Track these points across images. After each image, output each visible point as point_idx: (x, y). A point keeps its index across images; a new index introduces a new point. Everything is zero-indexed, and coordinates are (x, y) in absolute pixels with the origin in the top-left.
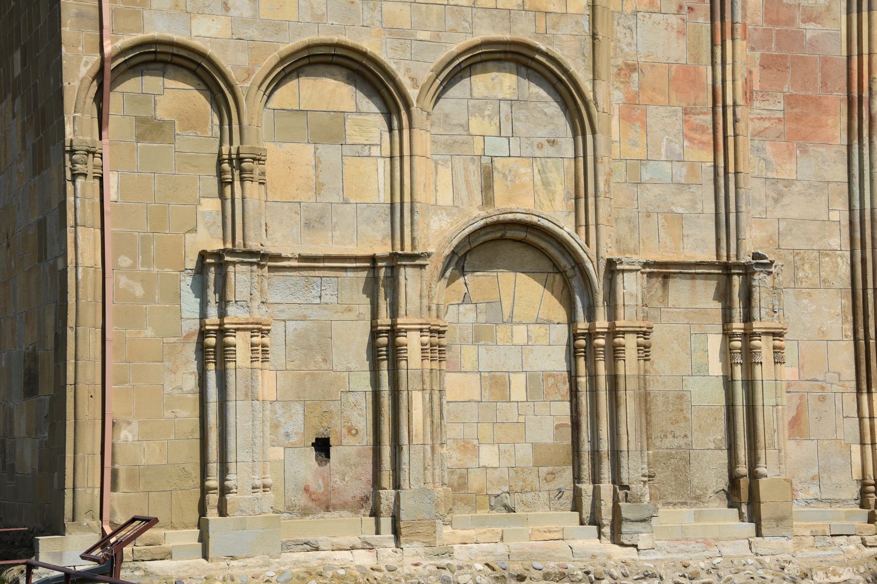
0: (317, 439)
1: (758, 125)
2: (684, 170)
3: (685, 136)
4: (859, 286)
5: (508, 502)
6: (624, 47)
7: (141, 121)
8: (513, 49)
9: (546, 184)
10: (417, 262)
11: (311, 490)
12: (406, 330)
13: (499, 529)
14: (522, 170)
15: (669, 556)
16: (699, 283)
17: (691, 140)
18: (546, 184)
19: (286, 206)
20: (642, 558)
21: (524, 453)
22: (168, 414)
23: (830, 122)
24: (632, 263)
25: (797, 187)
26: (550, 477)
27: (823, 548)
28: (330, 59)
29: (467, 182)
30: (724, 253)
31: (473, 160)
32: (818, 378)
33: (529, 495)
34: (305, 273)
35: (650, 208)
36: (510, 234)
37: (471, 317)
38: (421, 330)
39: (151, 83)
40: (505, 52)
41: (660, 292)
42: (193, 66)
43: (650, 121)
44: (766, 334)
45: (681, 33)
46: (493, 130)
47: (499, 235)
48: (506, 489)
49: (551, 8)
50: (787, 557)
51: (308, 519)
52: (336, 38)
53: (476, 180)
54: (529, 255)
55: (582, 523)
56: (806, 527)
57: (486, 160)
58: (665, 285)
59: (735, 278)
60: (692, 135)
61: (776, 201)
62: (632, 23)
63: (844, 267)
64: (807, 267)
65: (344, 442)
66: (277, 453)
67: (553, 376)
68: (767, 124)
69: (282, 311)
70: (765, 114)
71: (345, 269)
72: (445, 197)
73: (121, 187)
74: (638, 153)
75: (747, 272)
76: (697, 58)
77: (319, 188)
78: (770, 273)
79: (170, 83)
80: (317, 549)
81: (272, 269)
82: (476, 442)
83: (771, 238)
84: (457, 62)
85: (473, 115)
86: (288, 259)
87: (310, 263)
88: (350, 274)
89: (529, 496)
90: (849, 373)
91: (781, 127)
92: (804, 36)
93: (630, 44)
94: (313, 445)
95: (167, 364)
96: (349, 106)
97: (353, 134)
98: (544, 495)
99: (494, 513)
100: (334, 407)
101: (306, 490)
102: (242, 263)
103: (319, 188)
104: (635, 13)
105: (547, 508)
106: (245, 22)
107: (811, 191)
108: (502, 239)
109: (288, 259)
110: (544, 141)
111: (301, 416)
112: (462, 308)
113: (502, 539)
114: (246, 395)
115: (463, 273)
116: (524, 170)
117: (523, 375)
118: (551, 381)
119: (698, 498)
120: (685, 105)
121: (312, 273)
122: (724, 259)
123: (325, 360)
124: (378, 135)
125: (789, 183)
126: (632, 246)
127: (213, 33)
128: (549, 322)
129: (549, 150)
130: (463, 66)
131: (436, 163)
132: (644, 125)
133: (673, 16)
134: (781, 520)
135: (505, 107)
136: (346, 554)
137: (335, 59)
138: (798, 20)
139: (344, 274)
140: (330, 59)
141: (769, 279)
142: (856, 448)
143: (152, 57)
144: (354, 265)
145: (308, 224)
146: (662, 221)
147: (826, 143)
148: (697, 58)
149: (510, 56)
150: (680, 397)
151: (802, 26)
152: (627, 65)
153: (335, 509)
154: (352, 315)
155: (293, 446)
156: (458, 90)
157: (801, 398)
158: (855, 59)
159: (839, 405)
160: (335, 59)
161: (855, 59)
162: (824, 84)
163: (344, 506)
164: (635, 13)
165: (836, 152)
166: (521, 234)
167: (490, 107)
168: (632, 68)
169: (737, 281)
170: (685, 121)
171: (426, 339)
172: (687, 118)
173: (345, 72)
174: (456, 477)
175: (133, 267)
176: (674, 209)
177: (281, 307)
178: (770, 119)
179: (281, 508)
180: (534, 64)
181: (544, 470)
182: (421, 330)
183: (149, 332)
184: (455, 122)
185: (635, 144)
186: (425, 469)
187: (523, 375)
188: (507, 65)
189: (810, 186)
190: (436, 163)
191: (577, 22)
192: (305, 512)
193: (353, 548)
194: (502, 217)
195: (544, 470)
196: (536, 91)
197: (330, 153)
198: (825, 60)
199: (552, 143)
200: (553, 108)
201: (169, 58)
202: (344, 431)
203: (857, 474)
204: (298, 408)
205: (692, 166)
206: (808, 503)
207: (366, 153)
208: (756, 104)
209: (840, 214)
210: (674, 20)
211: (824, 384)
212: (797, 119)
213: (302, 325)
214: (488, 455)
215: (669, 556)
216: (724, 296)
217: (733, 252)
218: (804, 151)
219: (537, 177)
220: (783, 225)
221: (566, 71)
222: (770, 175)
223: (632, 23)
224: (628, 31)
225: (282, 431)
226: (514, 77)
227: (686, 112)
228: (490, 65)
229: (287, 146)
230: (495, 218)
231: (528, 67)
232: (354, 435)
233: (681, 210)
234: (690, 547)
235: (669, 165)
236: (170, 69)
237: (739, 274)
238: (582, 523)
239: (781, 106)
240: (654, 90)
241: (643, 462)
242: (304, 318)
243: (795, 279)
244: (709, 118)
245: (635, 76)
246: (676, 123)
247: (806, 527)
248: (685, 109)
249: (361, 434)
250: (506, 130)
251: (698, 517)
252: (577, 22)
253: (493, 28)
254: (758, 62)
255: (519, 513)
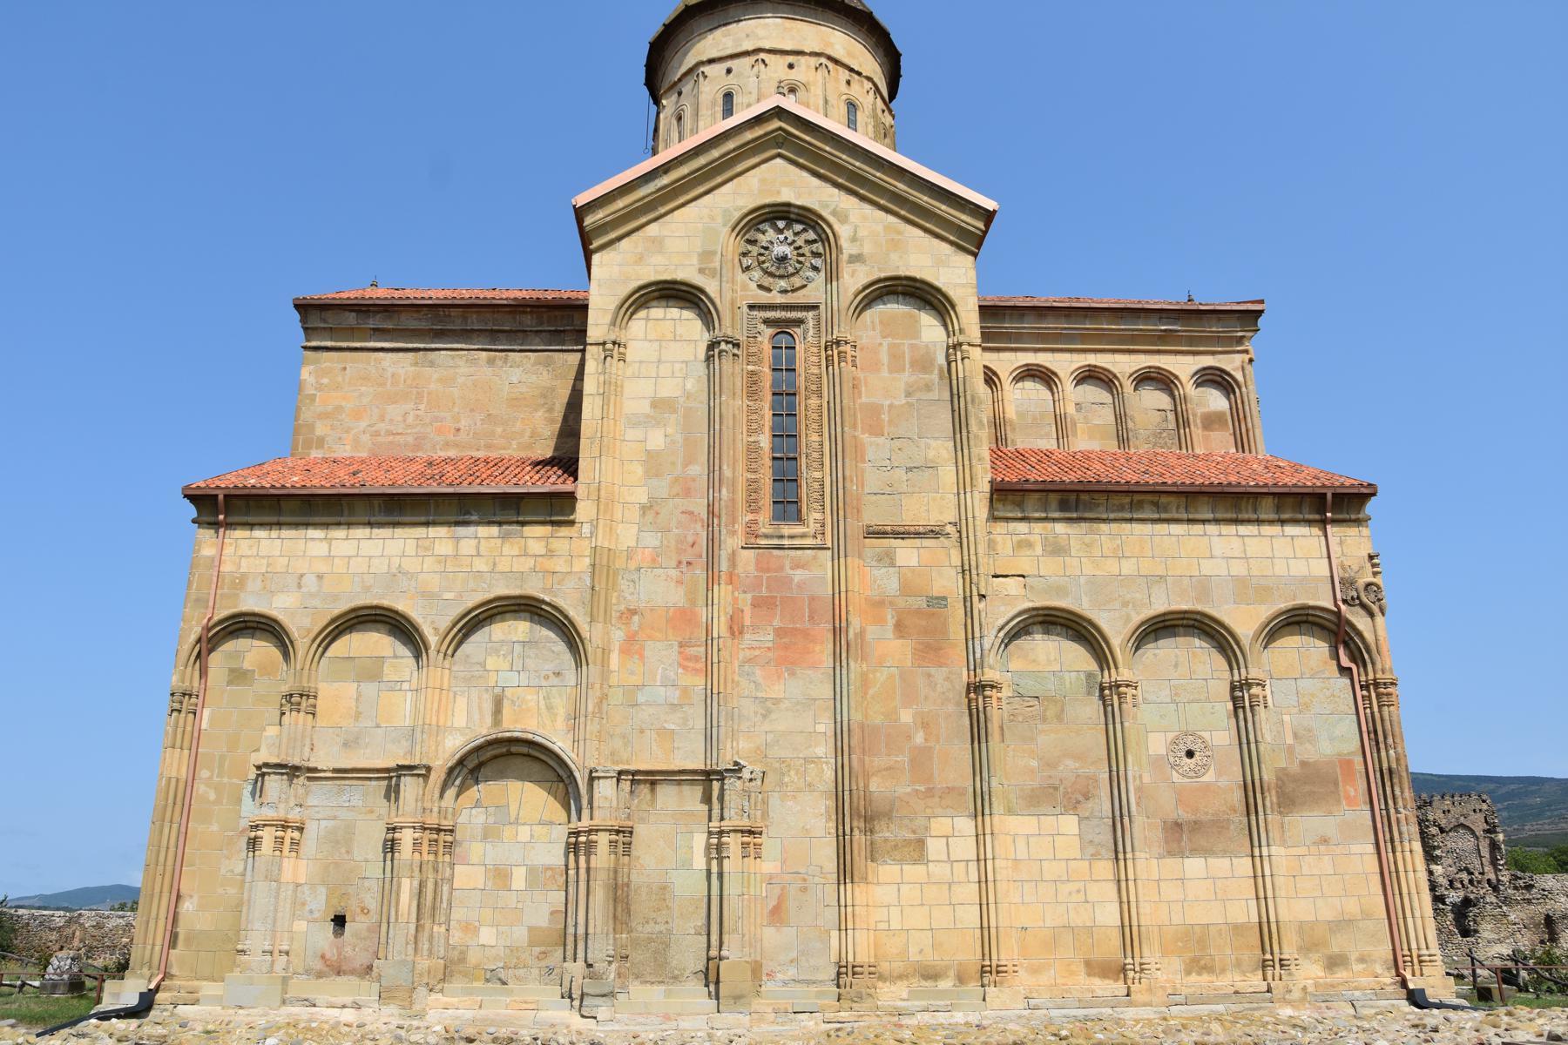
0: (335, 916)
1: (748, 653)
2: (678, 693)
3: (680, 665)
4: (840, 789)
5: (502, 976)
6: (627, 595)
7: (232, 671)
8: (523, 602)
9: (549, 708)
10: (415, 772)
11: (327, 957)
12: (401, 828)
13: (479, 998)
14: (529, 697)
15: (626, 1028)
16: (686, 789)
17: (685, 668)
18: (549, 708)
19: (331, 730)
20: (600, 1028)
21: (520, 934)
22: (220, 891)
23: (818, 648)
24: (608, 771)
25: (786, 704)
26: (542, 956)
27: (783, 1024)
28: (373, 618)
29: (480, 708)
30: (709, 762)
31: (487, 690)
32: (801, 871)
33: (521, 971)
34: (338, 782)
35: (644, 726)
36: (514, 749)
37: (482, 819)
38: (414, 828)
39: (242, 644)
40: (519, 605)
41: (649, 797)
42: (271, 629)
43: (647, 653)
44: (735, 831)
45: (679, 582)
46: (506, 666)
47: (504, 750)
48: (501, 965)
49: (558, 569)
50: (739, 1031)
51: (321, 980)
52: (375, 602)
53: (488, 707)
54: (536, 767)
55: (563, 997)
56: (768, 1005)
57: (497, 690)
58: (653, 791)
59: (715, 782)
60: (686, 663)
61: (764, 716)
62: (635, 577)
63: (829, 773)
64: (792, 773)
65: (357, 919)
66: (301, 926)
67: (550, 869)
68: (757, 652)
69: (318, 812)
70: (755, 644)
71: (370, 779)
72: (460, 720)
73: (211, 719)
74: (635, 680)
75: (721, 775)
76: (693, 602)
77: (358, 715)
78: (740, 778)
79: (256, 643)
80: (314, 1006)
81: (309, 779)
82: (477, 924)
83: (758, 748)
84: (473, 614)
85: (490, 655)
86: (324, 771)
87: (341, 773)
88: (374, 783)
89: (521, 972)
90: (831, 866)
91: (770, 654)
92: (792, 580)
93: (633, 593)
94: (332, 920)
95: (225, 852)
96: (388, 652)
97: (389, 673)
98: (535, 972)
99: (490, 985)
100: (351, 890)
101: (323, 957)
102: (274, 773)
103: (358, 715)
104: (639, 569)
105: (537, 983)
106: (311, 595)
107: (798, 707)
108: (510, 754)
109: (324, 771)
110: (550, 673)
111: (324, 897)
112: (474, 811)
113: (480, 1007)
114: (266, 877)
115: (477, 782)
116: (531, 697)
117: (525, 868)
118: (549, 873)
119: (675, 978)
120: (680, 639)
121: (343, 782)
122: (709, 767)
123: (348, 852)
124: (409, 673)
125: (777, 701)
126: (625, 758)
127: (287, 605)
128: (552, 823)
129: (554, 680)
130: (481, 617)
131: (455, 694)
132: (642, 657)
133: (674, 571)
134: (737, 998)
135: (518, 648)
136: (336, 1012)
137: (378, 618)
138: (787, 568)
139: (368, 783)
140: (373, 618)
141: (739, 783)
142: (835, 934)
143: (242, 625)
144: (376, 775)
145: (346, 744)
146: (654, 736)
147: (814, 667)
148: (693, 602)
149: (522, 607)
150: (664, 888)
151: (792, 572)
152: (629, 610)
153: (345, 973)
154: (374, 816)
155: (315, 921)
156: (478, 637)
157: (783, 889)
158: (837, 595)
159: (820, 895)
160: (378, 618)
161: (837, 595)
162: (811, 618)
163: (353, 972)
164: (639, 569)
165: (823, 674)
166: (525, 750)
167: (505, 648)
168: (633, 612)
169: (716, 785)
170: (680, 653)
171: (417, 835)
172: (682, 650)
173: (388, 627)
174: (456, 953)
175: (211, 778)
176: (666, 725)
177: (317, 809)
178: (760, 648)
179: (301, 971)
180: (542, 613)
181: (537, 950)
182: (414, 828)
183: (215, 827)
184: (474, 661)
185: (632, 673)
186: (407, 943)
187: (525, 868)
188: (522, 615)
189: (798, 703)
190: (455, 694)
191: (580, 579)
192: (320, 975)
193: (344, 1007)
194: (500, 735)
195: (537, 950)
196: (546, 633)
197: (369, 689)
198: (812, 599)
199: (558, 674)
200: (560, 646)
201: (255, 625)
202: (358, 910)
203: (834, 958)
204: (322, 891)
205: (685, 691)
206: (785, 983)
207: (398, 688)
208: (747, 636)
209: (825, 726)
210: (674, 573)
211: (806, 877)
212: (786, 647)
213: (331, 824)
214: (487, 936)
215: (626, 1028)
216: (707, 799)
217: (714, 761)
218: (793, 674)
219: (542, 703)
220: (770, 737)
221: (566, 617)
222: (759, 695)
223: (635, 577)
224: (631, 584)
225: (307, 908)
226: (528, 624)
227: (681, 645)
228: (508, 615)
229: (336, 685)
230: (494, 736)
231: (540, 616)
232: (366, 914)
233: (673, 727)
234: (648, 1021)
235: (663, 689)
236: (258, 633)
237: (718, 780)
238: (563, 997)
239: (771, 637)
240: (652, 628)
241: (608, 944)
242: (335, 818)
243: (781, 784)
244: (703, 649)
245: (636, 618)
246: (673, 654)
247: (768, 1005)
248: (680, 643)
249: (371, 913)
250: (518, 665)
251: (668, 994)
252: (580, 579)
253: (507, 587)
254: (749, 602)
255: (511, 986)
